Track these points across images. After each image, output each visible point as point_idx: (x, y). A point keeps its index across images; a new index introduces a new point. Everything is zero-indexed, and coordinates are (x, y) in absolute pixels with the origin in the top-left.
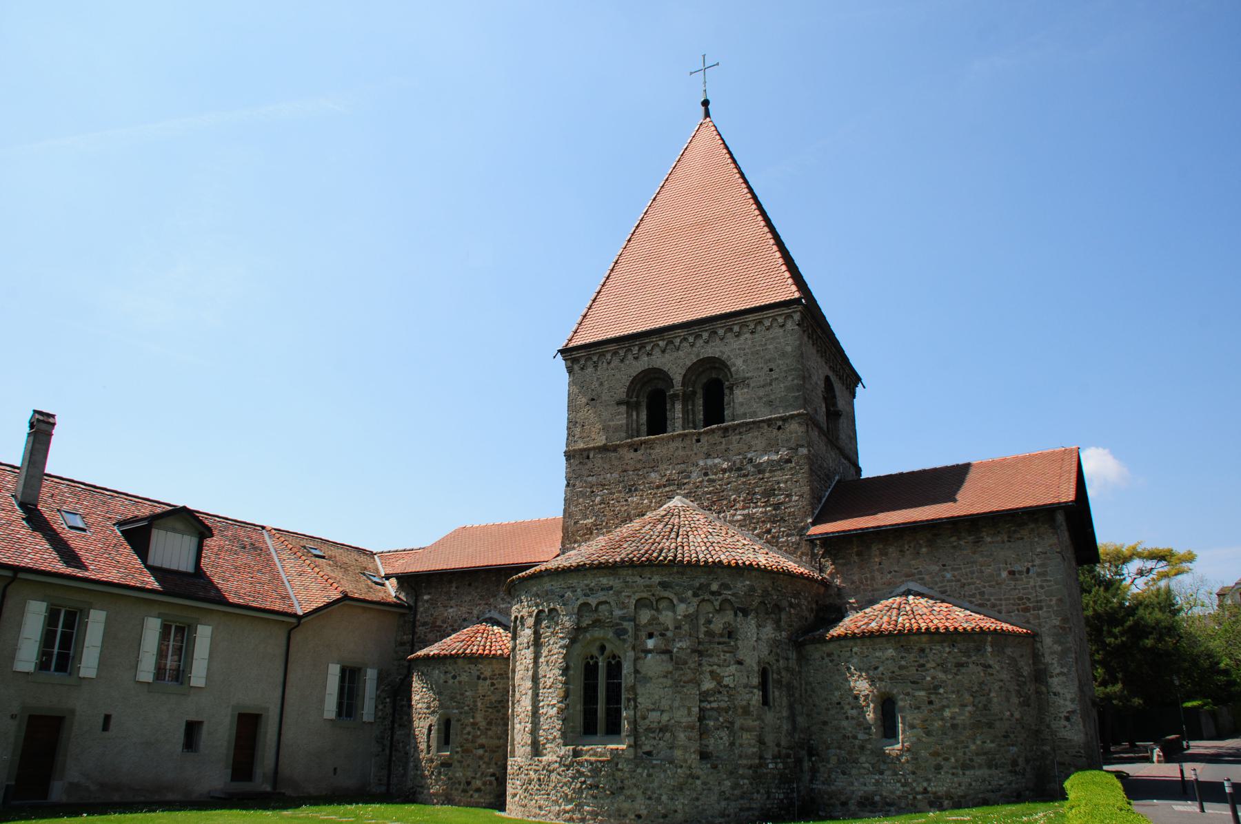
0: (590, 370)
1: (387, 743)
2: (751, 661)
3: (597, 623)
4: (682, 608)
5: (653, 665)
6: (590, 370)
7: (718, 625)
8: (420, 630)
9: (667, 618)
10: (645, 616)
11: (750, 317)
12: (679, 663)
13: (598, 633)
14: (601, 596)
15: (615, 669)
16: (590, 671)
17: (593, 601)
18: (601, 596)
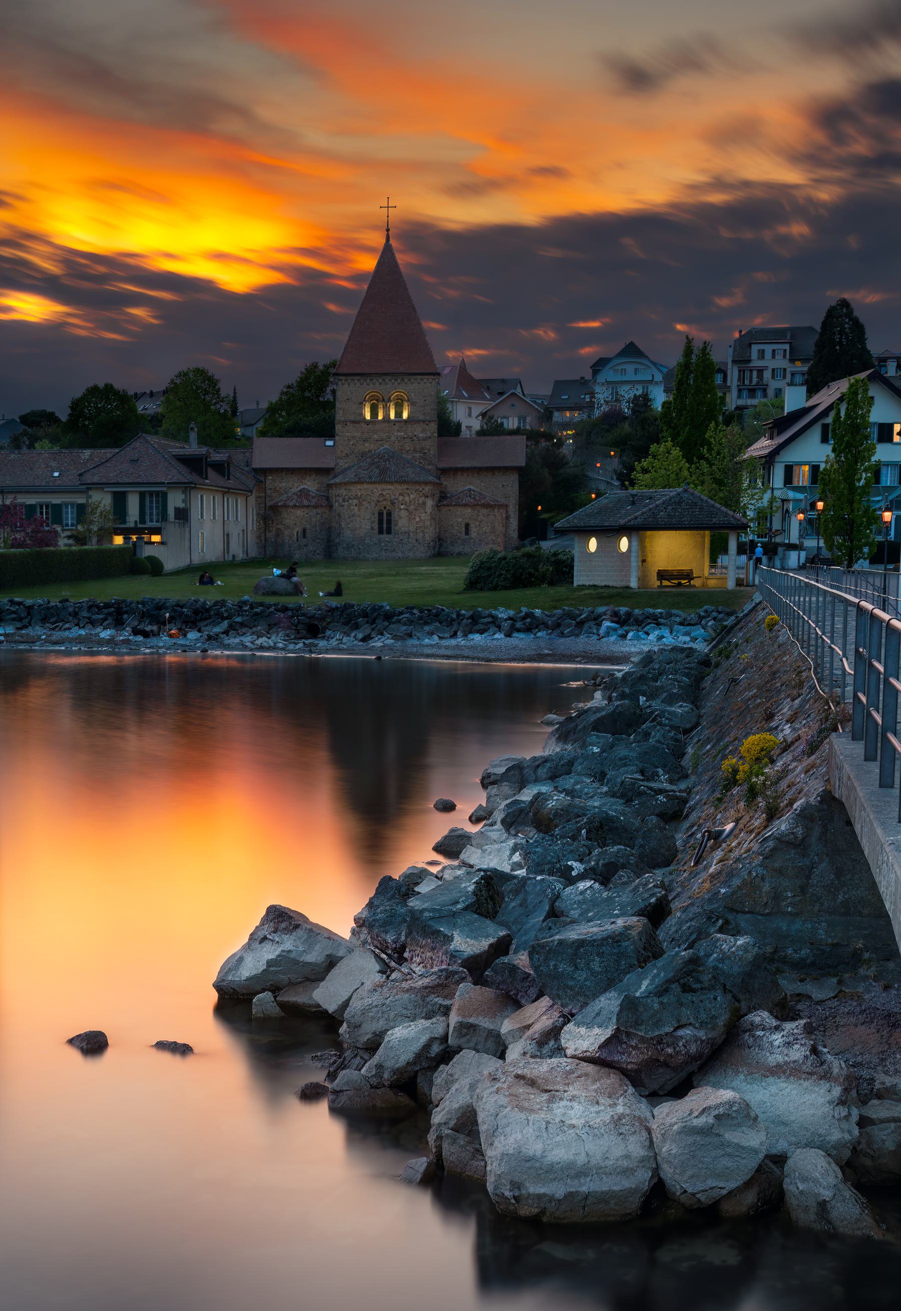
0: (346, 386)
1: (263, 539)
2: (429, 512)
3: (385, 500)
4: (412, 496)
5: (403, 513)
6: (346, 386)
7: (420, 501)
8: (268, 492)
9: (407, 499)
10: (401, 498)
11: (419, 377)
12: (411, 513)
13: (385, 503)
14: (388, 492)
15: (389, 514)
16: (381, 514)
17: (384, 493)
18: (388, 492)
